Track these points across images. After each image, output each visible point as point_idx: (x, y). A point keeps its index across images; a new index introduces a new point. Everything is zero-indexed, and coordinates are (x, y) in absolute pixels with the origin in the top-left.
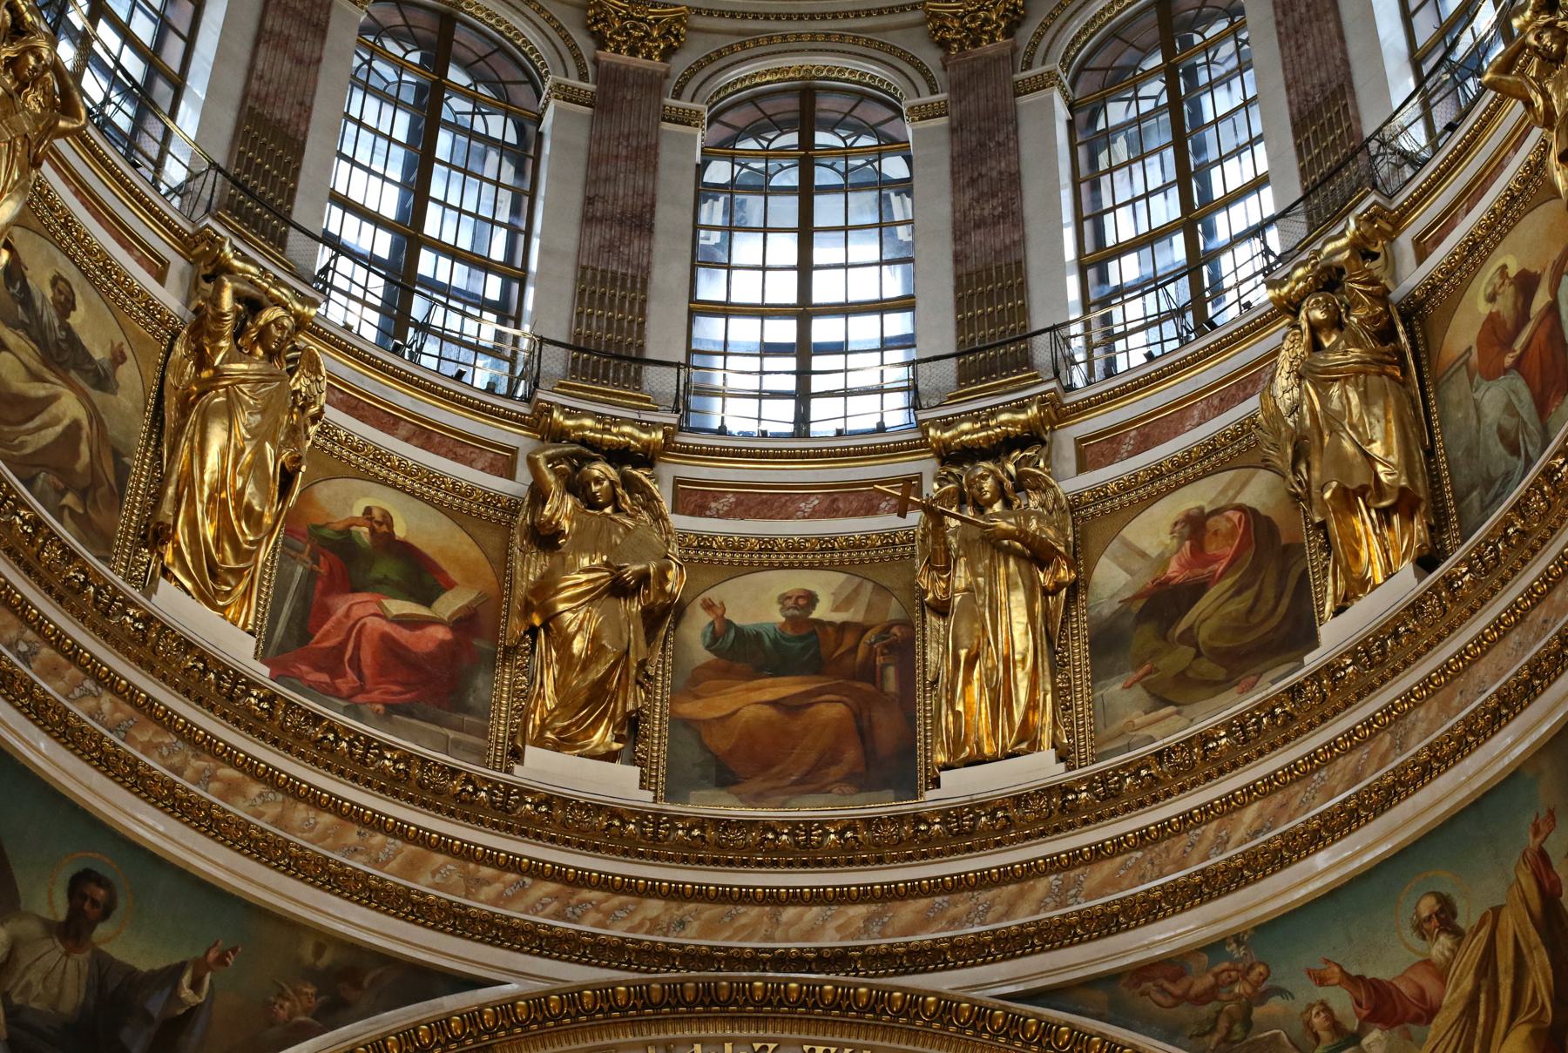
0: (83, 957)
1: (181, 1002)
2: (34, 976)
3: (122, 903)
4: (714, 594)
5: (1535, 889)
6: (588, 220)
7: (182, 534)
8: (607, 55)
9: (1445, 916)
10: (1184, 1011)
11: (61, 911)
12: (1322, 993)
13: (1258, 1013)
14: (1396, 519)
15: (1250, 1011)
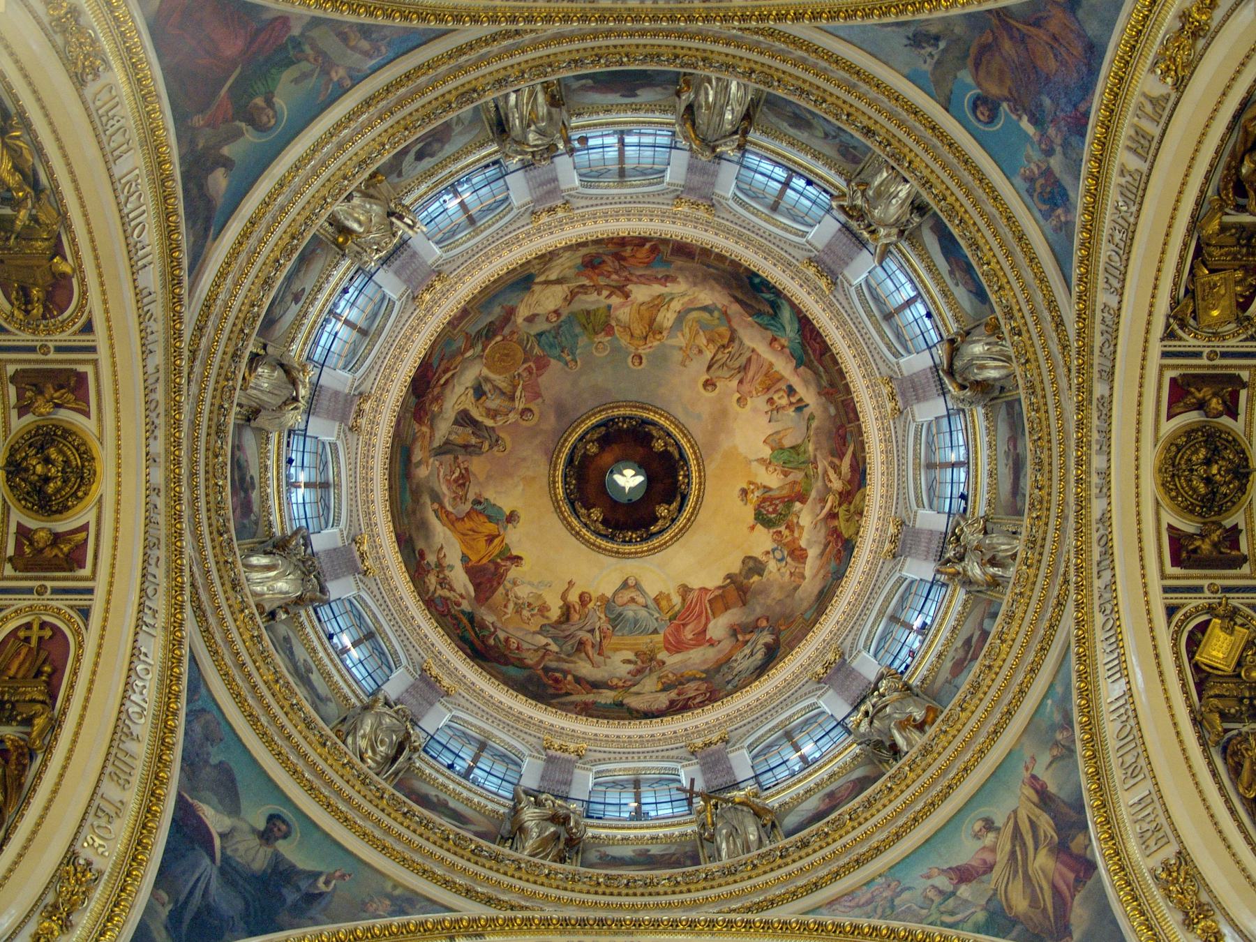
0: (269, 850)
1: (317, 888)
2: (241, 847)
3: (297, 834)
4: (602, 849)
5: (1032, 792)
6: (543, 778)
7: (350, 740)
8: (551, 752)
9: (989, 825)
10: (857, 911)
11: (261, 825)
12: (930, 882)
13: (897, 902)
14: (927, 728)
15: (892, 901)
